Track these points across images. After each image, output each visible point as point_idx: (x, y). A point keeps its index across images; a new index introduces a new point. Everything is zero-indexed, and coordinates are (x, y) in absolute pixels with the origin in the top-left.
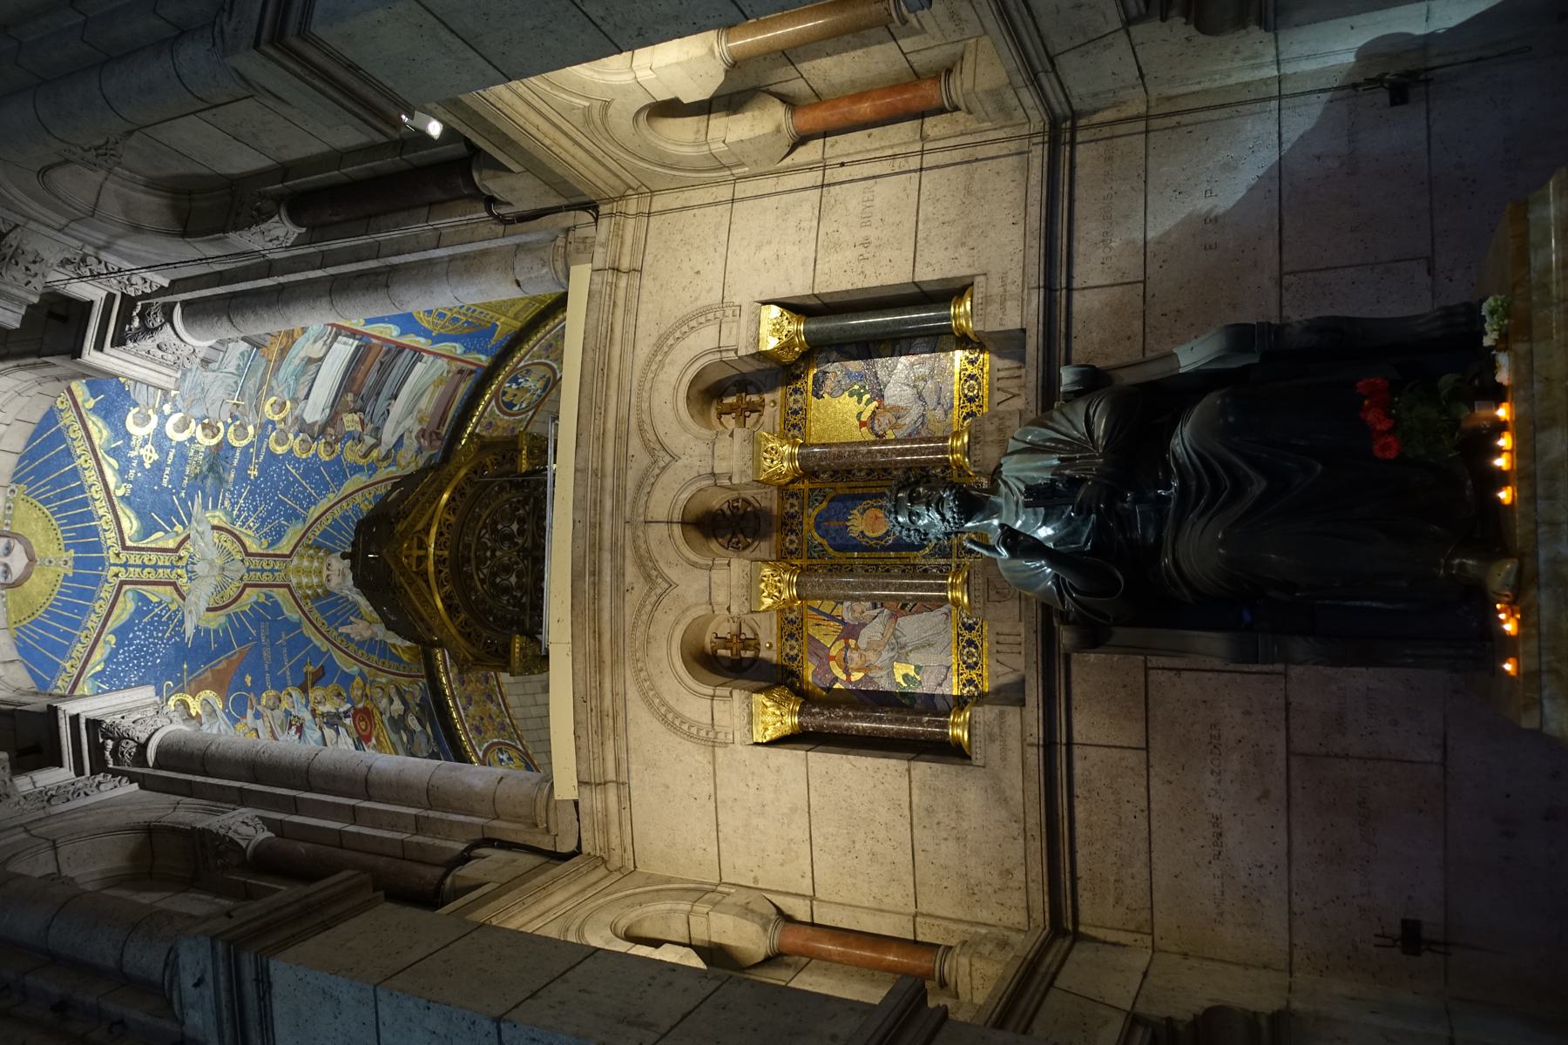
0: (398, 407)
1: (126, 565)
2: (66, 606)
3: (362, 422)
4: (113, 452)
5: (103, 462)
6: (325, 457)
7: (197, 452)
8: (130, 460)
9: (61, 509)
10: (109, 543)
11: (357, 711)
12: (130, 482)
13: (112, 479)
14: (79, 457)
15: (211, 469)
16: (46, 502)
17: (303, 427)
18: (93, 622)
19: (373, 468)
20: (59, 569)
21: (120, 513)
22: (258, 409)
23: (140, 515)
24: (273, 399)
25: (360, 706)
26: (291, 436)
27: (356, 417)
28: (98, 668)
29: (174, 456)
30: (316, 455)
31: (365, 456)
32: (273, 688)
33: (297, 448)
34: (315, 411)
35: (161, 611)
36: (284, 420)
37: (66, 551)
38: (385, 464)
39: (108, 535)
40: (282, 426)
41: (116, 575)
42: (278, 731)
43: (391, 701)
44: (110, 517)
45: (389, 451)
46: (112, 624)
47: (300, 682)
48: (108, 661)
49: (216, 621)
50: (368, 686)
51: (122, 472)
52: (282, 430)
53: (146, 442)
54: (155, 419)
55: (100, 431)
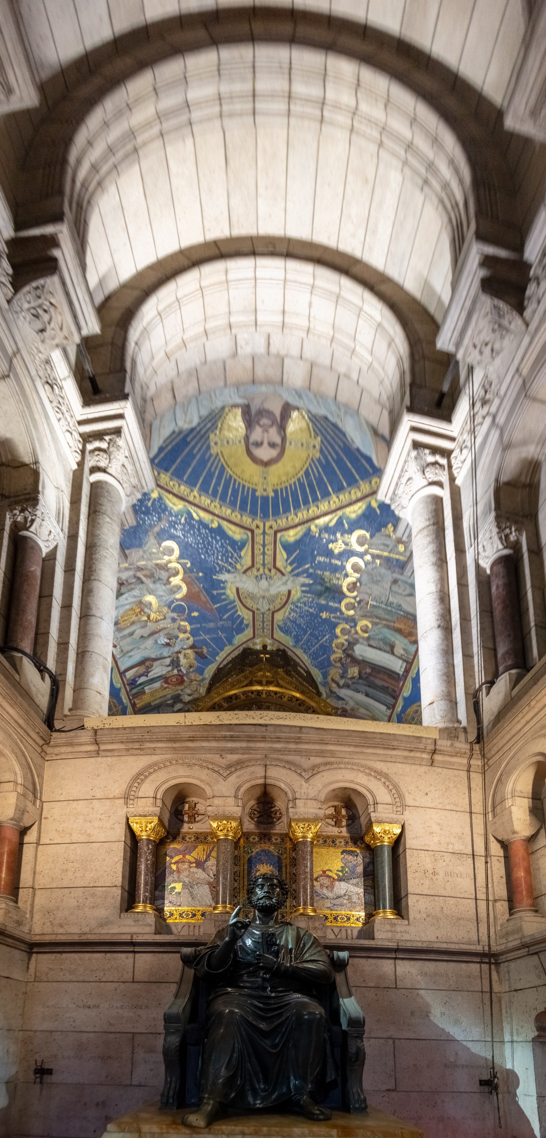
0: (361, 697)
1: (264, 533)
2: (235, 492)
3: (353, 678)
4: (340, 522)
5: (334, 515)
6: (333, 657)
7: (338, 579)
8: (334, 534)
9: (302, 485)
10: (279, 521)
11: (182, 677)
12: (320, 535)
13: (322, 521)
14: (338, 497)
15: (327, 589)
16: (307, 474)
17: (351, 644)
18: (227, 512)
19: (325, 684)
20: (260, 485)
21: (299, 528)
22: (364, 617)
23: (299, 543)
24: (370, 625)
25: (185, 678)
26: (346, 637)
27: (356, 674)
28: (195, 515)
29: (336, 565)
30: (334, 652)
31: (333, 680)
32: (192, 629)
33: (339, 641)
34: (361, 651)
35: (236, 558)
36: (357, 633)
37: (273, 491)
38: (328, 691)
39: (284, 520)
40: (353, 631)
41: (258, 527)
42: (166, 632)
43: (189, 695)
44: (297, 521)
45: (335, 693)
46: (225, 524)
47: (197, 644)
48: (201, 522)
49: (231, 593)
50: (197, 683)
51: (326, 529)
52: (350, 632)
53: (346, 544)
54: (361, 549)
55: (354, 512)
